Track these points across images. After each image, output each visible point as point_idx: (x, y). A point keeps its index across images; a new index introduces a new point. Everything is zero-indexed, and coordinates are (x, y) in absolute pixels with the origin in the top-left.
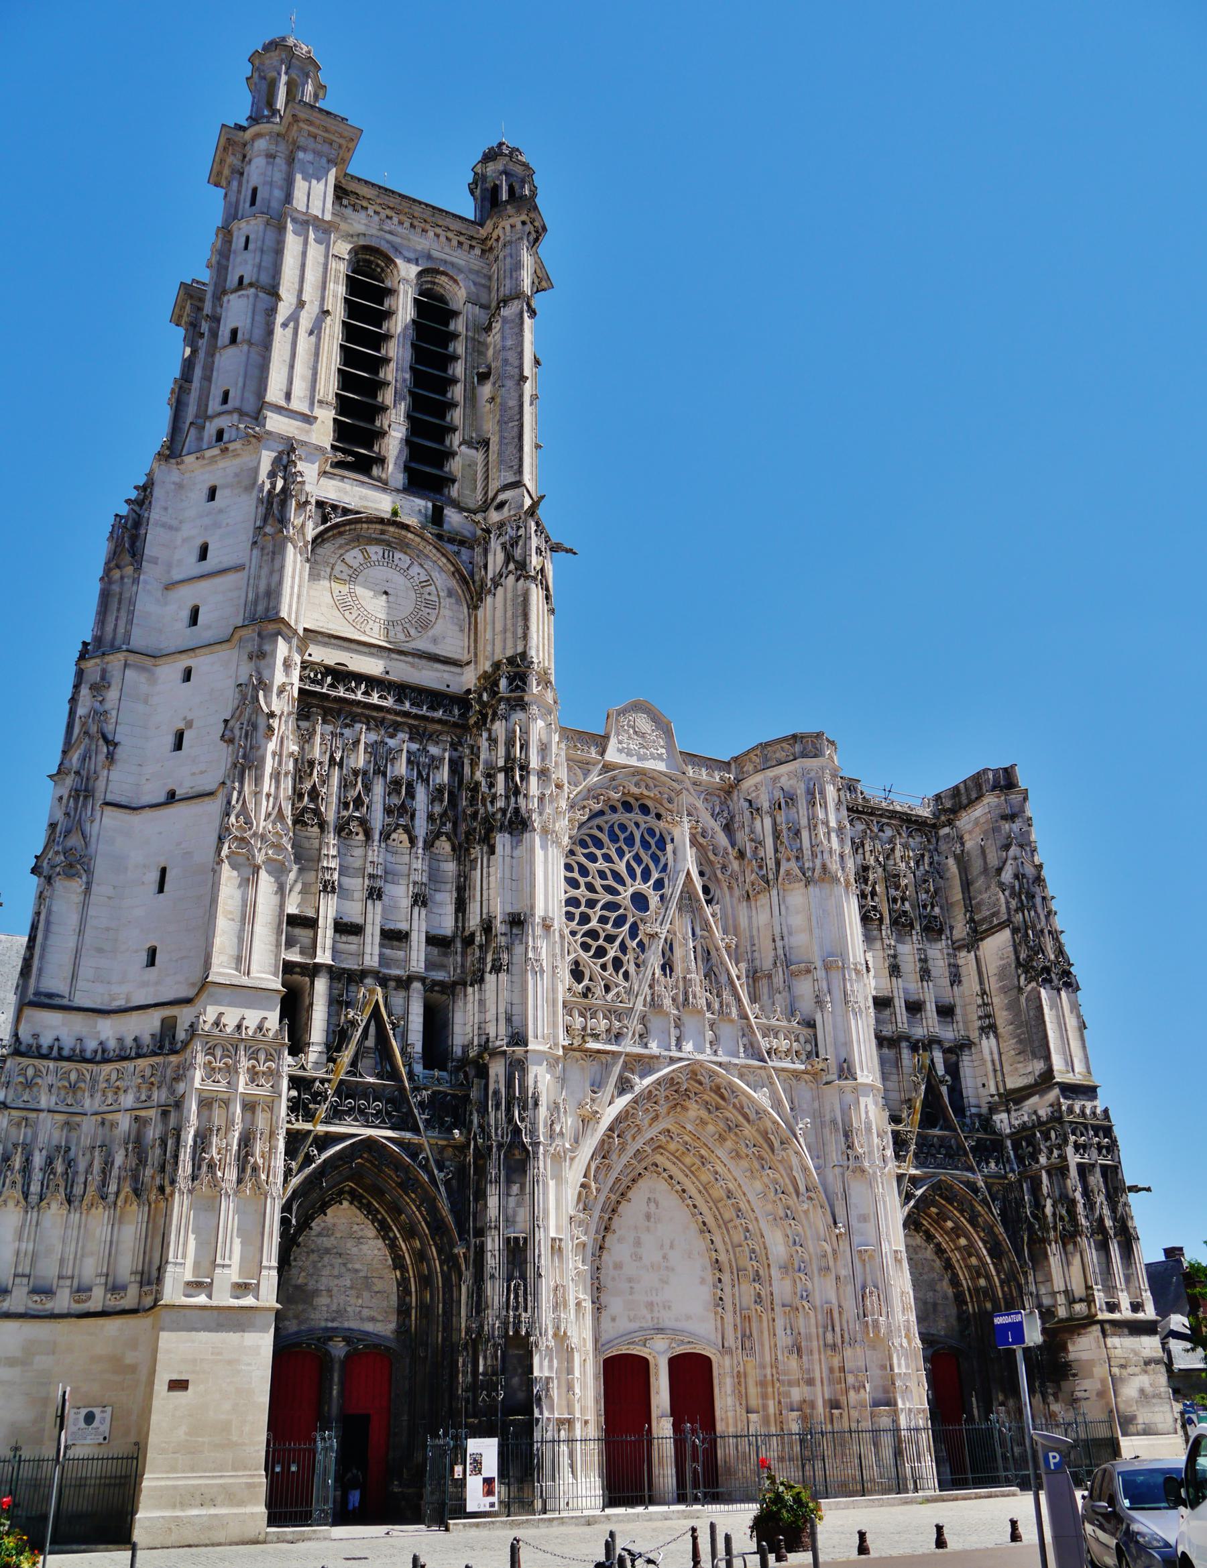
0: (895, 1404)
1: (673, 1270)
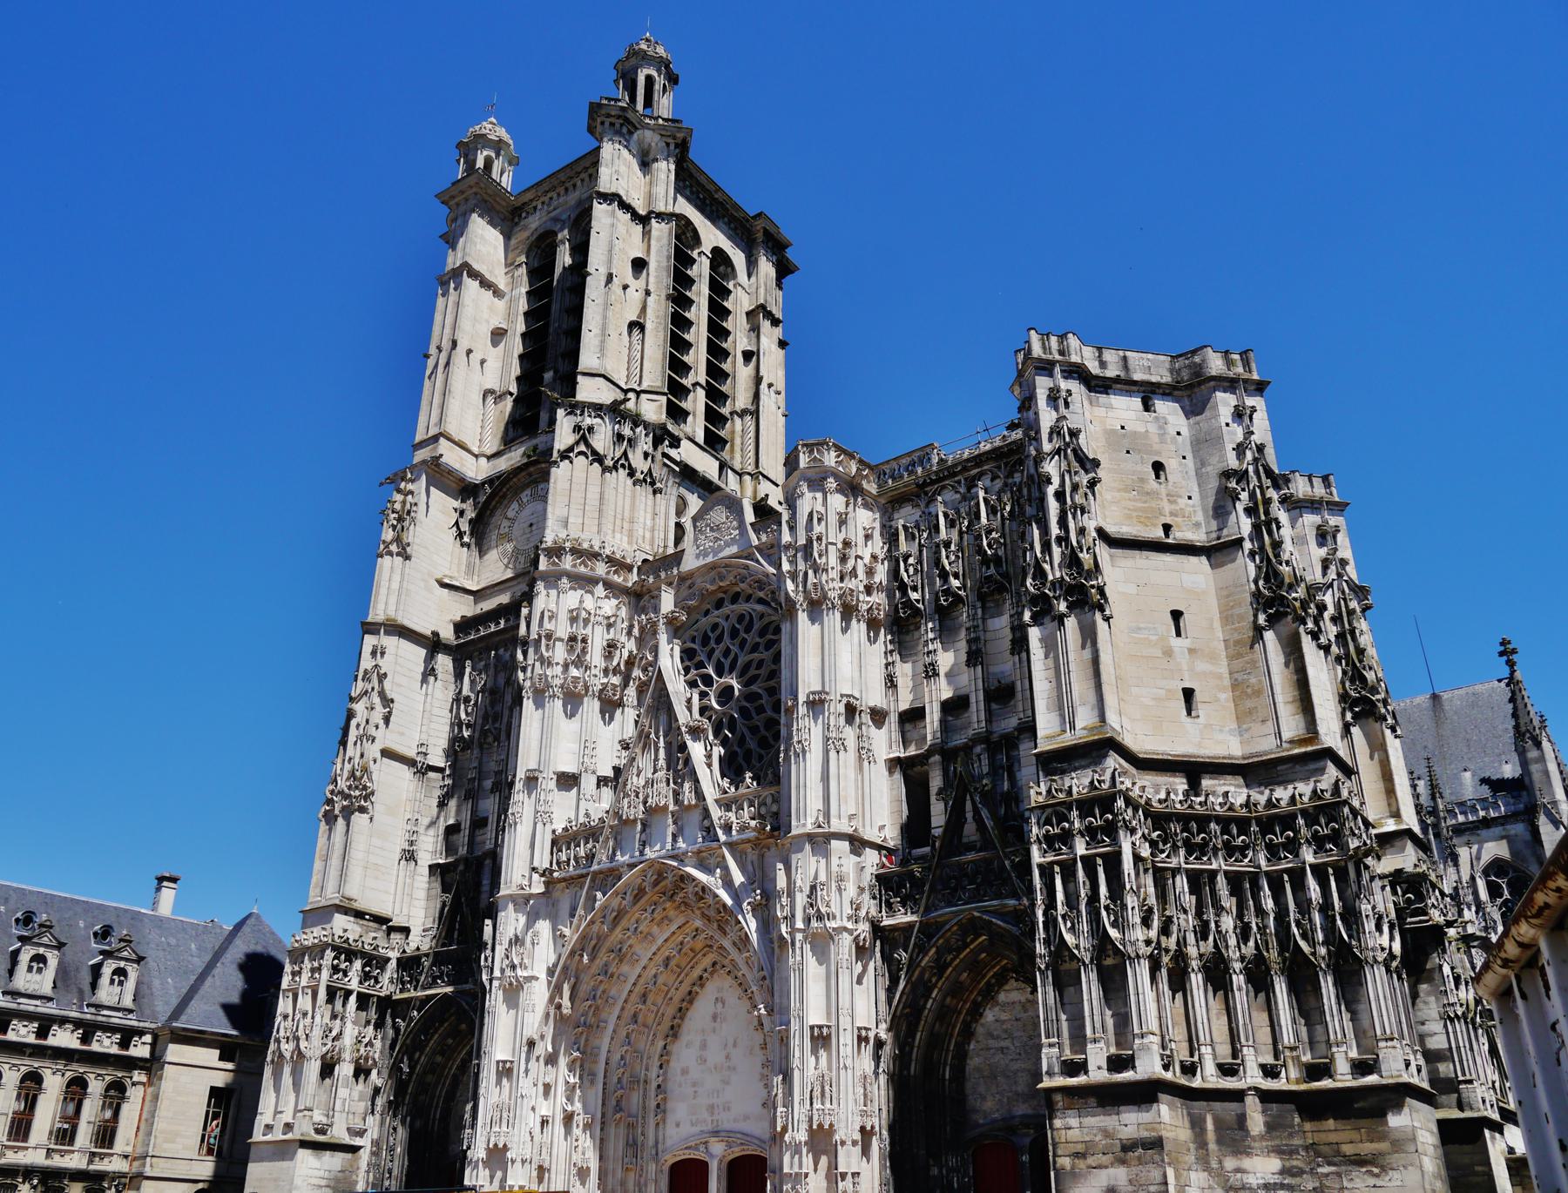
1: (734, 1069)
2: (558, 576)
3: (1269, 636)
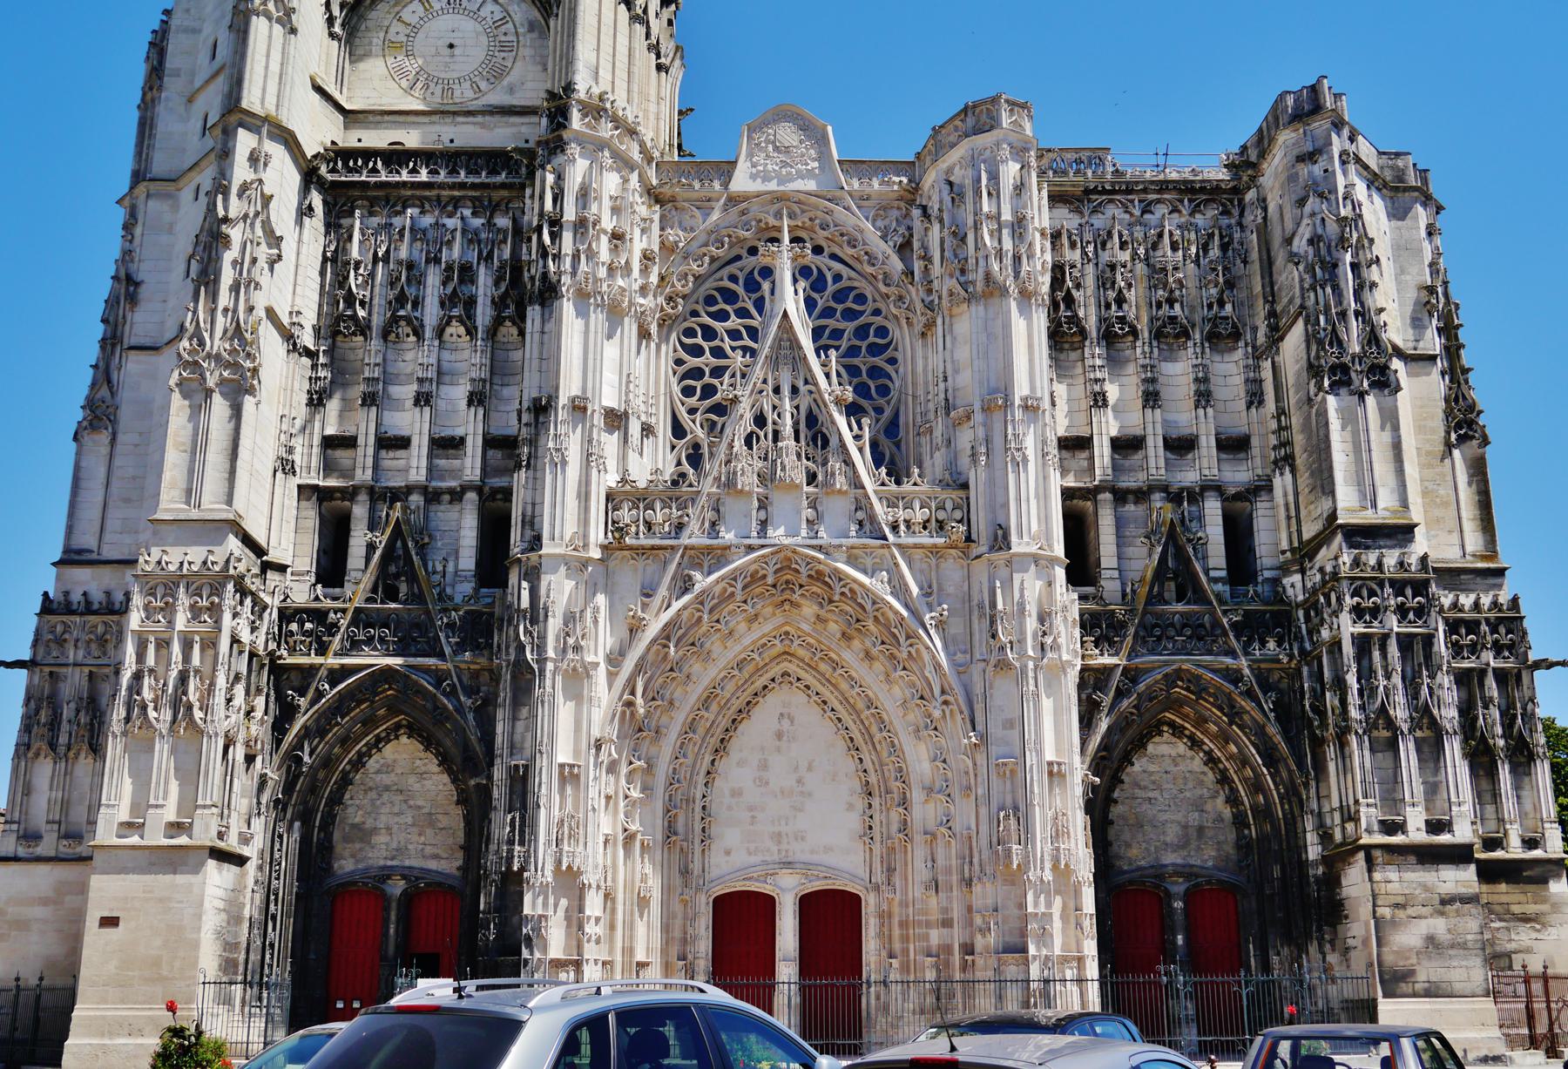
0: (1024, 950)
2: (601, 145)
3: (1456, 453)
